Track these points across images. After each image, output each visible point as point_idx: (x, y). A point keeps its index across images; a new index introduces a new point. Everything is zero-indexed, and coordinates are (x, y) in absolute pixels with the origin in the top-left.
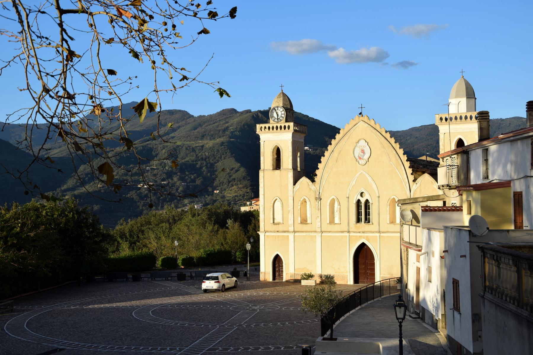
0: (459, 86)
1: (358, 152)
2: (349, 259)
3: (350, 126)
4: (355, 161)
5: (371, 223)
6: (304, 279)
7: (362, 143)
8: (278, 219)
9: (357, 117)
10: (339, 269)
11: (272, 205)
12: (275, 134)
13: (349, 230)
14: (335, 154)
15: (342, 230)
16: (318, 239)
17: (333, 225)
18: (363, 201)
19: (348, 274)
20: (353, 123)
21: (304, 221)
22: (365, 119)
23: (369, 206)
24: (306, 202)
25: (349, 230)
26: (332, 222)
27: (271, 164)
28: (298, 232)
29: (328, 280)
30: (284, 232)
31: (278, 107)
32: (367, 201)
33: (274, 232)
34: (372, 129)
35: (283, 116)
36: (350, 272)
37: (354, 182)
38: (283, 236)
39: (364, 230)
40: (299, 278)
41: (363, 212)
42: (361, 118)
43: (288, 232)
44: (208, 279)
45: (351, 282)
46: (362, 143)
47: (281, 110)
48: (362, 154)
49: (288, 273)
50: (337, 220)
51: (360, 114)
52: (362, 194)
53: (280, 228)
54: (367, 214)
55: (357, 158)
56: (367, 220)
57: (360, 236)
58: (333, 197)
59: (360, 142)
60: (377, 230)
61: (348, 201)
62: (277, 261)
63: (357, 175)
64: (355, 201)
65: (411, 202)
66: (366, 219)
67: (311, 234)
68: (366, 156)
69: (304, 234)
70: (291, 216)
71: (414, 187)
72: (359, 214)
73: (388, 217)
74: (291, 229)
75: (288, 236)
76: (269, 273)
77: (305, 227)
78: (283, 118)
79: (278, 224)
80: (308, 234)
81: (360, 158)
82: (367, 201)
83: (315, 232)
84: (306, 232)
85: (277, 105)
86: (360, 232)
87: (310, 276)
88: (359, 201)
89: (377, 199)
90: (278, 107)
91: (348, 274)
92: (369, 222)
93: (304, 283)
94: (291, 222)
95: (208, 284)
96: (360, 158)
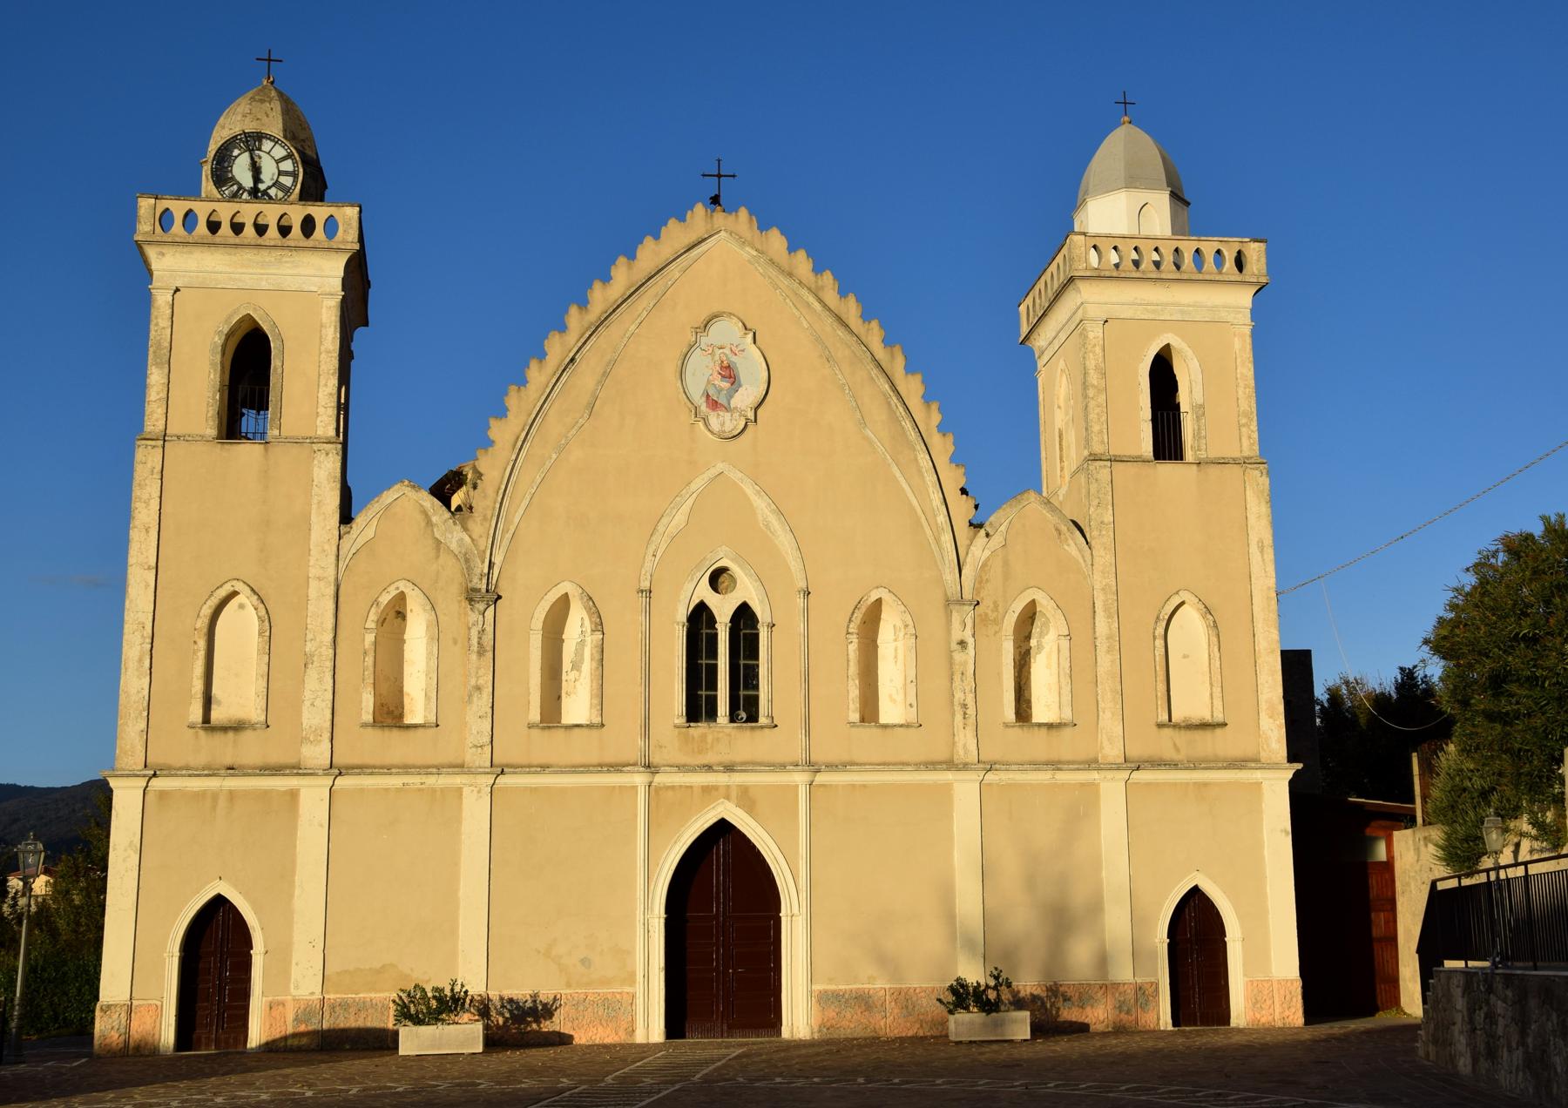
1: (702, 373)
2: (647, 907)
4: (686, 417)
5: (763, 720)
6: (417, 1021)
7: (726, 332)
8: (239, 695)
10: (585, 962)
11: (202, 623)
12: (248, 255)
14: (585, 377)
15: (610, 758)
18: (723, 609)
20: (675, 235)
21: (390, 714)
23: (754, 639)
24: (401, 615)
25: (646, 753)
27: (212, 411)
29: (519, 1027)
32: (744, 615)
33: (211, 771)
36: (647, 977)
37: (680, 518)
38: (266, 794)
39: (727, 758)
41: (721, 666)
42: (720, 218)
43: (296, 769)
47: (279, 152)
48: (725, 385)
49: (278, 1000)
50: (577, 706)
52: (717, 578)
53: (249, 749)
56: (746, 708)
57: (707, 790)
58: (566, 587)
59: (715, 329)
60: (799, 755)
61: (648, 612)
63: (698, 483)
64: (682, 615)
67: (431, 781)
68: (745, 397)
69: (395, 781)
70: (316, 687)
71: (979, 550)
74: (317, 754)
76: (159, 1010)
77: (394, 746)
79: (237, 727)
80: (414, 780)
81: (714, 405)
82: (744, 615)
83: (459, 767)
84: (406, 769)
86: (709, 768)
87: (447, 1005)
89: (800, 601)
90: (260, 137)
92: (753, 717)
93: (414, 1041)
94: (315, 715)
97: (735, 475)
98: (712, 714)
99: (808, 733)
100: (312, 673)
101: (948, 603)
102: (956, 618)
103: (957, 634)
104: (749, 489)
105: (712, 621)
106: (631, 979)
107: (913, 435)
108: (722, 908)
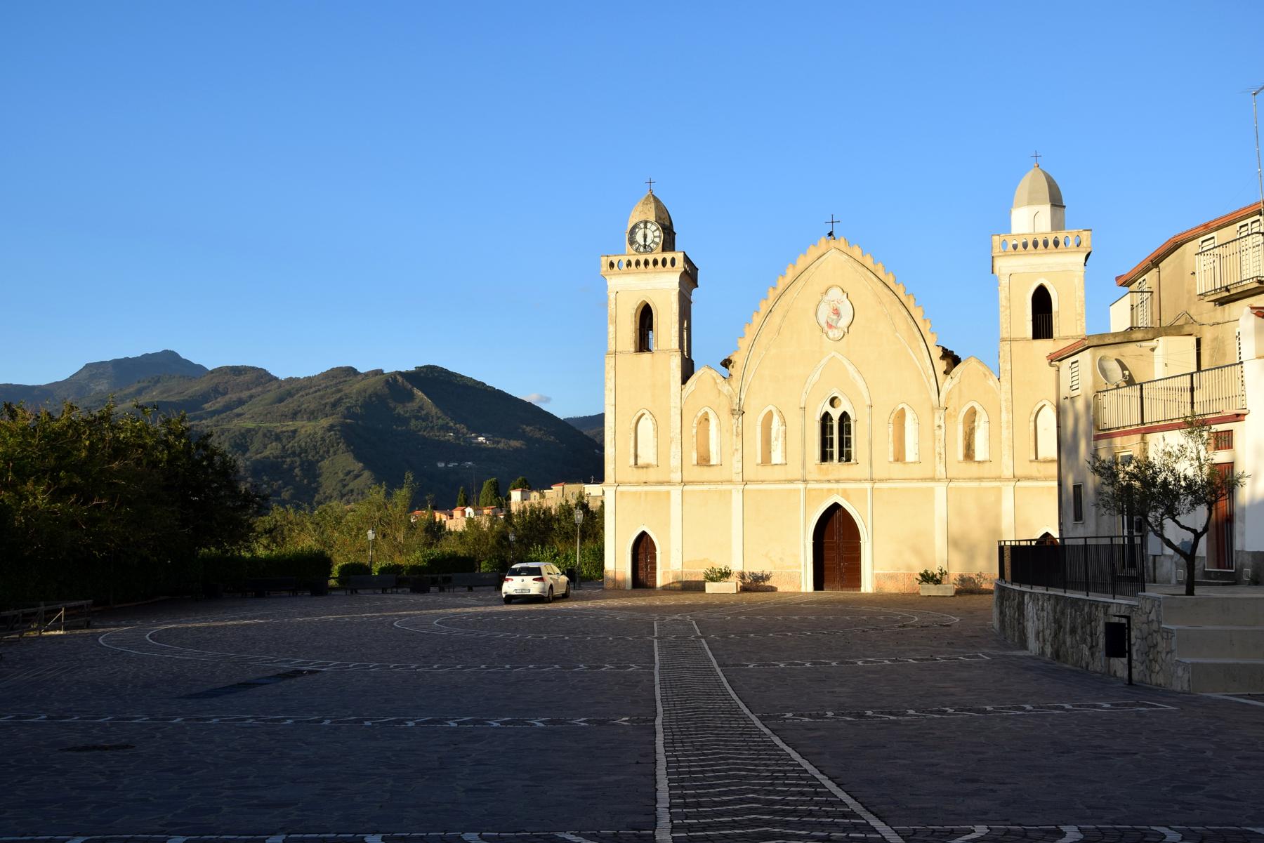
0: (1032, 181)
1: (825, 313)
2: (805, 538)
3: (809, 259)
4: (818, 332)
6: (712, 580)
7: (835, 294)
8: (646, 456)
9: (823, 239)
10: (781, 559)
11: (633, 426)
12: (643, 276)
13: (804, 476)
14: (776, 318)
15: (789, 477)
16: (737, 497)
17: (768, 468)
18: (836, 415)
19: (802, 570)
20: (813, 252)
21: (704, 461)
22: (841, 244)
24: (707, 420)
25: (804, 476)
26: (766, 460)
27: (632, 341)
28: (692, 482)
29: (754, 584)
30: (661, 483)
31: (646, 223)
32: (844, 417)
33: (638, 484)
34: (856, 265)
35: (657, 240)
36: (805, 565)
37: (817, 376)
38: (658, 493)
39: (836, 477)
40: (701, 578)
41: (835, 438)
42: (832, 243)
43: (669, 483)
44: (517, 573)
45: (807, 585)
46: (835, 294)
47: (654, 228)
49: (667, 569)
50: (777, 457)
51: (830, 234)
53: (652, 475)
54: (845, 442)
55: (825, 326)
56: (845, 456)
57: (829, 490)
58: (771, 407)
59: (830, 293)
60: (867, 476)
62: (643, 548)
64: (818, 417)
65: (1117, 340)
66: (841, 454)
67: (720, 487)
69: (706, 487)
70: (675, 450)
72: (825, 443)
73: (891, 449)
74: (676, 477)
75: (668, 492)
77: (705, 473)
78: (657, 244)
79: (647, 467)
80: (712, 487)
81: (830, 326)
82: (844, 417)
83: (730, 482)
84: (710, 482)
85: (643, 218)
87: (726, 574)
88: (827, 414)
89: (868, 410)
90: (646, 223)
91: (802, 570)
92: (848, 460)
93: (711, 588)
94: (675, 462)
95: (512, 586)
96: (830, 326)
97: (839, 357)
98: (832, 458)
99: (871, 466)
100: (673, 446)
101: (933, 409)
102: (937, 416)
103: (937, 422)
104: (845, 362)
105: (831, 419)
106: (799, 567)
107: (918, 335)
108: (835, 538)
